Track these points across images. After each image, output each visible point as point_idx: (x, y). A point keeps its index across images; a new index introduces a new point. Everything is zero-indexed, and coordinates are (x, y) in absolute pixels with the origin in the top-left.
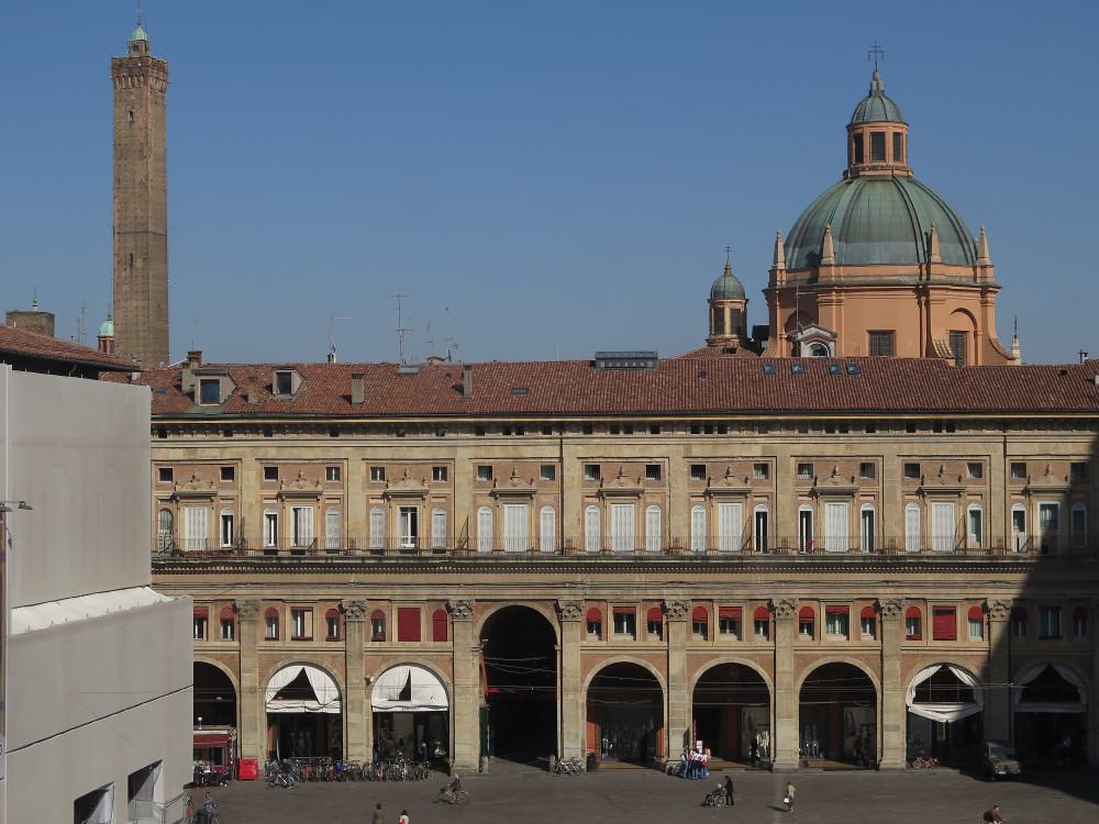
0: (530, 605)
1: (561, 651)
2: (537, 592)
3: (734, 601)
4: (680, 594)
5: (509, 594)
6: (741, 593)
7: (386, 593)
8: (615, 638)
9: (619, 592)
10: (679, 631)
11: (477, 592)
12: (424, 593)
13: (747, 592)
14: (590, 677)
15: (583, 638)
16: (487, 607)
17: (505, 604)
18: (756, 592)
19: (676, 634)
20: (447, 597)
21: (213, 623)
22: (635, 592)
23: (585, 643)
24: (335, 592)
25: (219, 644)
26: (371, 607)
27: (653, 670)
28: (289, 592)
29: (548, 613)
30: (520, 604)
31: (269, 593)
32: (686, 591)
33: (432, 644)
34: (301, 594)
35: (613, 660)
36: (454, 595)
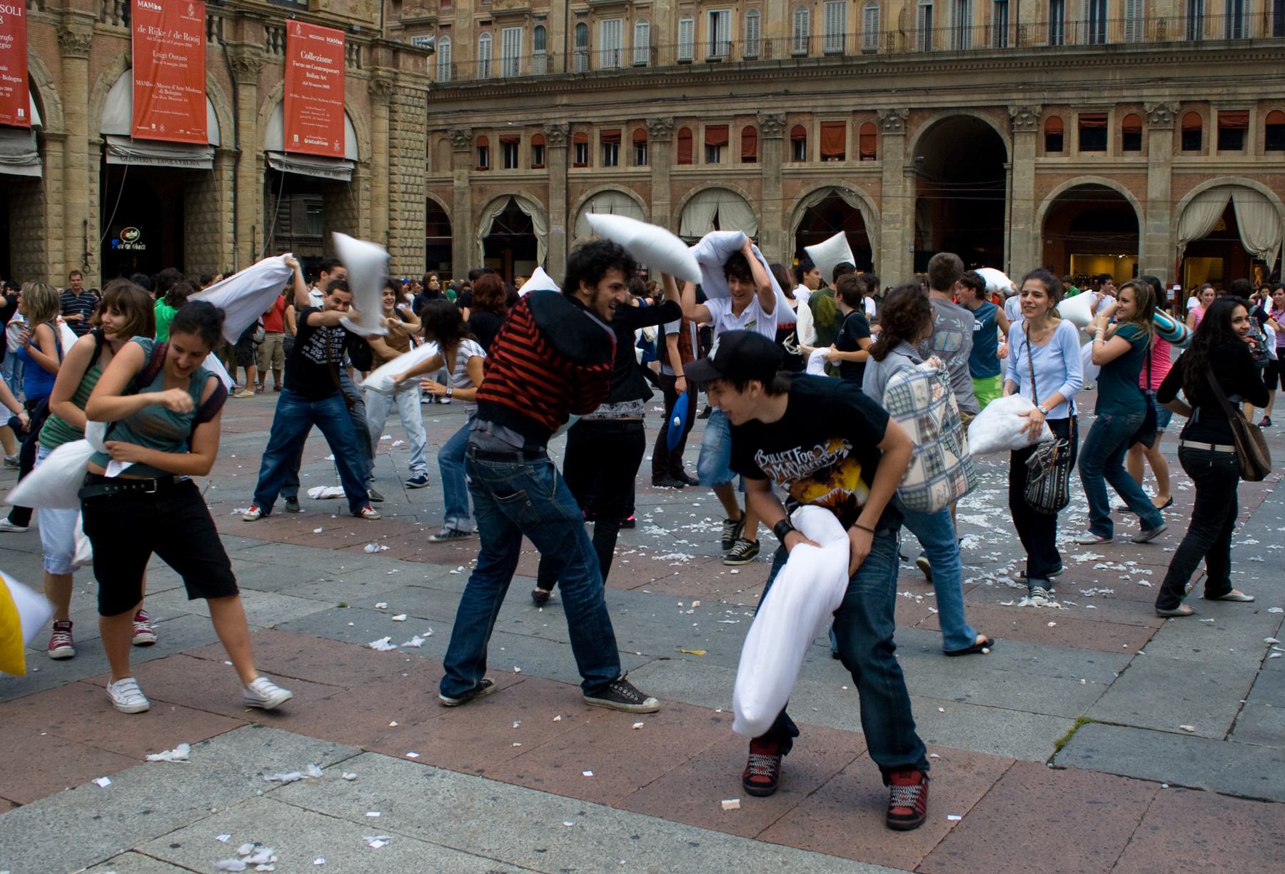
0: (976, 114)
1: (1012, 169)
2: (984, 97)
3: (1239, 102)
4: (1166, 95)
5: (950, 100)
6: (1248, 92)
7: (807, 104)
8: (1073, 154)
9: (1086, 94)
10: (1161, 144)
11: (911, 99)
12: (850, 103)
13: (1258, 90)
14: (1044, 206)
15: (1038, 155)
16: (924, 119)
17: (951, 113)
18: (1269, 89)
19: (1159, 148)
20: (875, 107)
21: (625, 148)
22: (1106, 94)
23: (1041, 160)
24: (750, 106)
25: (632, 169)
26: (793, 122)
27: (1128, 194)
28: (702, 108)
29: (994, 122)
30: (963, 112)
31: (682, 110)
32: (1174, 91)
33: (858, 163)
34: (719, 110)
35: (1076, 181)
36: (883, 103)
